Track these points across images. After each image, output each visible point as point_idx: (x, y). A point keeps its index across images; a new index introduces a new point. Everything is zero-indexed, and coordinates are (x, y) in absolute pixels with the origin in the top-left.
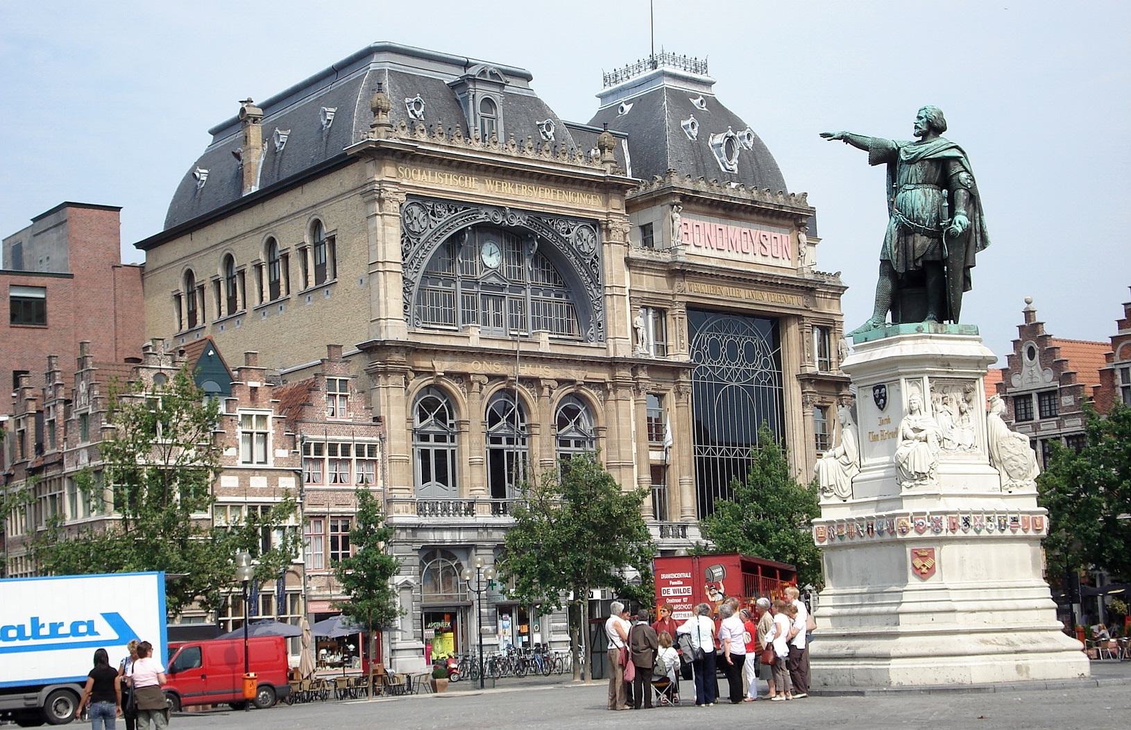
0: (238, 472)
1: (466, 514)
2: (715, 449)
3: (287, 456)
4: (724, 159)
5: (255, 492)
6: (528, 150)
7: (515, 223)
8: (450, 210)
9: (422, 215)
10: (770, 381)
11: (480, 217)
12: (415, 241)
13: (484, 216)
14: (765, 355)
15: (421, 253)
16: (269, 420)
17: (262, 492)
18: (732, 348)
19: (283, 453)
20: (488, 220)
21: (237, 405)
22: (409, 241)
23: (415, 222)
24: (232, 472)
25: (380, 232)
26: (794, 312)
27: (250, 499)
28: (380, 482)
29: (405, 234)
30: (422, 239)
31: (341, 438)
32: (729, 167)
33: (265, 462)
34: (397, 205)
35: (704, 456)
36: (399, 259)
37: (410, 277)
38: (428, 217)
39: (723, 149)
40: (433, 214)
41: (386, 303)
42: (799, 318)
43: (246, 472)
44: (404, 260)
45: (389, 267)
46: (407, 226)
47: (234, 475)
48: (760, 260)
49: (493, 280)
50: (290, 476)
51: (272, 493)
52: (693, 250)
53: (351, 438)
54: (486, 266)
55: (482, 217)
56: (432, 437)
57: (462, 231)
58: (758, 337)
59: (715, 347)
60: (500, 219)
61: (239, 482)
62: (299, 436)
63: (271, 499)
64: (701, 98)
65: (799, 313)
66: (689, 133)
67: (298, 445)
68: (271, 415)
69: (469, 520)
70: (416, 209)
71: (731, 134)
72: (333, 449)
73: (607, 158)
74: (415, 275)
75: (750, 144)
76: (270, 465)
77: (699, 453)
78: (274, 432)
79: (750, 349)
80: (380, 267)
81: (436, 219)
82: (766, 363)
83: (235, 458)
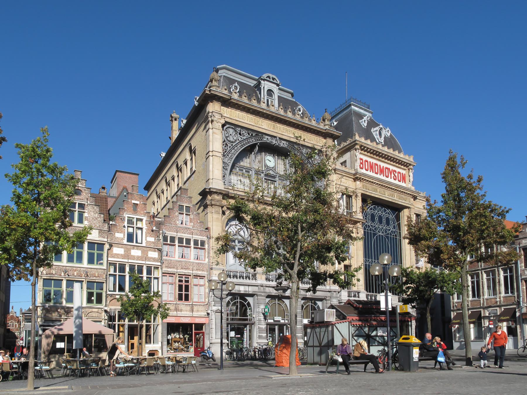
0: (124, 246)
1: (252, 279)
2: (372, 261)
3: (153, 241)
4: (378, 136)
5: (133, 258)
6: (289, 113)
7: (282, 145)
8: (249, 134)
9: (234, 133)
10: (396, 236)
11: (264, 139)
12: (230, 145)
13: (266, 139)
14: (394, 223)
15: (233, 151)
16: (144, 221)
17: (138, 258)
18: (380, 218)
19: (152, 239)
20: (268, 142)
21: (125, 211)
22: (226, 144)
23: (231, 137)
24: (120, 246)
25: (211, 137)
26: (407, 205)
27: (130, 261)
28: (207, 260)
29: (225, 141)
30: (234, 144)
31: (185, 236)
32: (380, 141)
33: (142, 243)
34: (221, 125)
35: (367, 263)
36: (221, 151)
37: (226, 160)
38: (237, 135)
39: (378, 132)
40: (240, 134)
41: (213, 171)
42: (409, 208)
43: (129, 247)
44: (224, 153)
45: (214, 153)
46: (227, 137)
47: (122, 248)
48: (392, 181)
49: (271, 172)
50: (155, 251)
51: (144, 259)
52: (364, 171)
53: (191, 236)
54: (267, 166)
55: (266, 139)
56: (237, 241)
57: (256, 144)
58: (391, 216)
59: (373, 216)
60: (274, 142)
61: (125, 251)
62: (161, 232)
63: (144, 262)
64: (368, 116)
65: (409, 206)
66: (363, 124)
67: (161, 236)
68: (145, 219)
69: (254, 282)
70: (231, 131)
71: (381, 126)
72: (181, 240)
73: (326, 124)
74: (229, 161)
75: (389, 135)
76: (144, 244)
77: (365, 262)
78: (146, 228)
79: (388, 220)
80: (211, 154)
81: (242, 137)
82: (394, 227)
83: (123, 239)
